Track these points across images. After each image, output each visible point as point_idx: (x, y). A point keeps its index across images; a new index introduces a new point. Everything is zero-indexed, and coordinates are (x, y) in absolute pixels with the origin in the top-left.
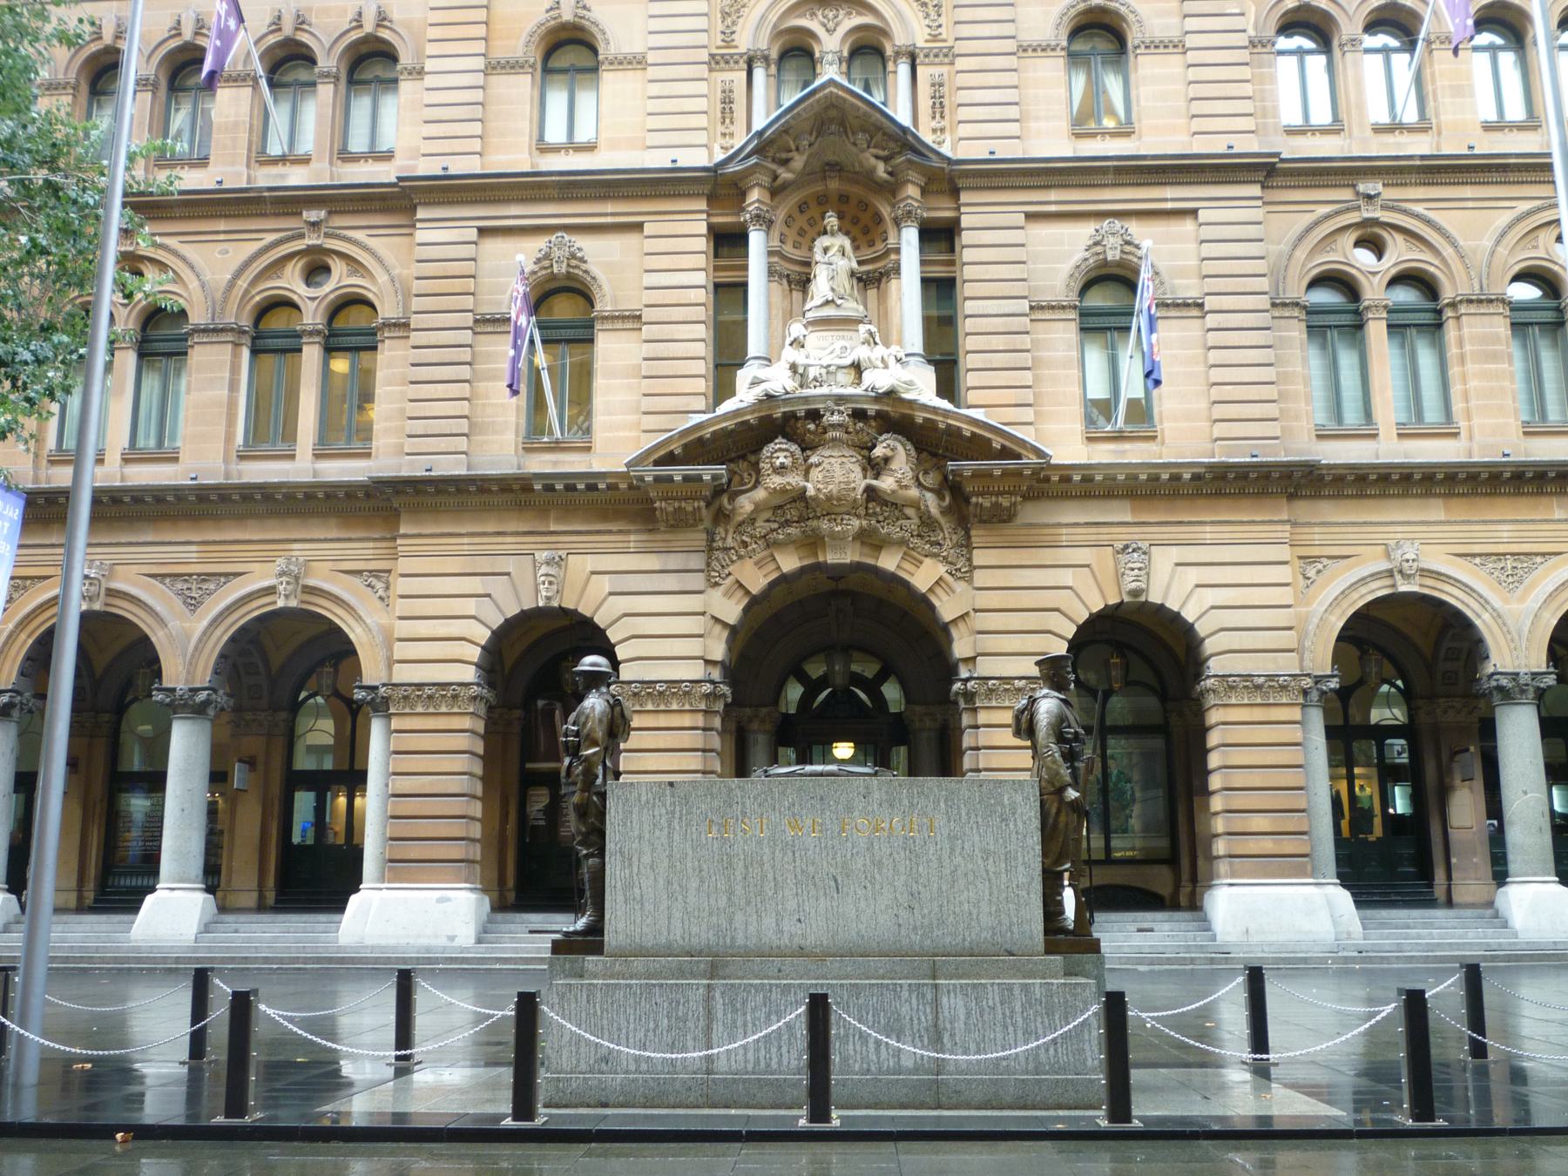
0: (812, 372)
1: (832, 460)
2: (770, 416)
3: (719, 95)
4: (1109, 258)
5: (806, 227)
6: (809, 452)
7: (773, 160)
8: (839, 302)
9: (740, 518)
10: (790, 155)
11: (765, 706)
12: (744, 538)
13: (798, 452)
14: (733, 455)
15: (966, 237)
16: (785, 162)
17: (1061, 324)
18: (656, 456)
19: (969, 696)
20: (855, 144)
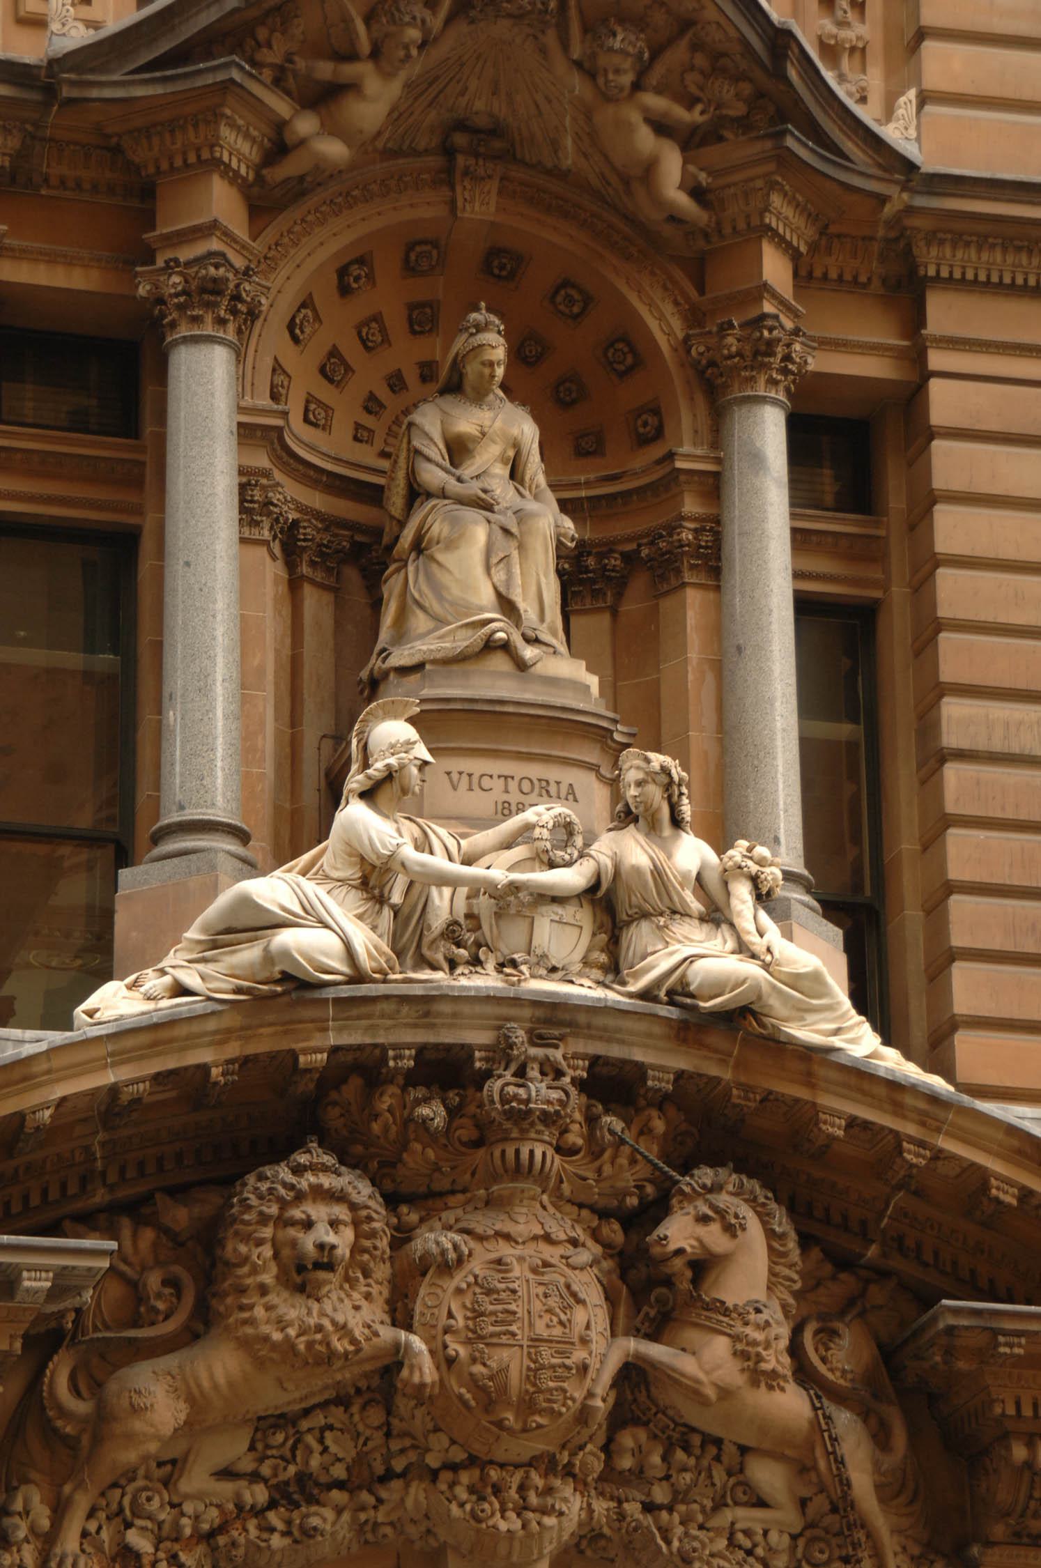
0: (442, 904)
1: (504, 1250)
2: (294, 1055)
5: (352, 350)
7: (278, 82)
9: (130, 1456)
10: (349, 70)
14: (100, 1197)
20: (587, 69)
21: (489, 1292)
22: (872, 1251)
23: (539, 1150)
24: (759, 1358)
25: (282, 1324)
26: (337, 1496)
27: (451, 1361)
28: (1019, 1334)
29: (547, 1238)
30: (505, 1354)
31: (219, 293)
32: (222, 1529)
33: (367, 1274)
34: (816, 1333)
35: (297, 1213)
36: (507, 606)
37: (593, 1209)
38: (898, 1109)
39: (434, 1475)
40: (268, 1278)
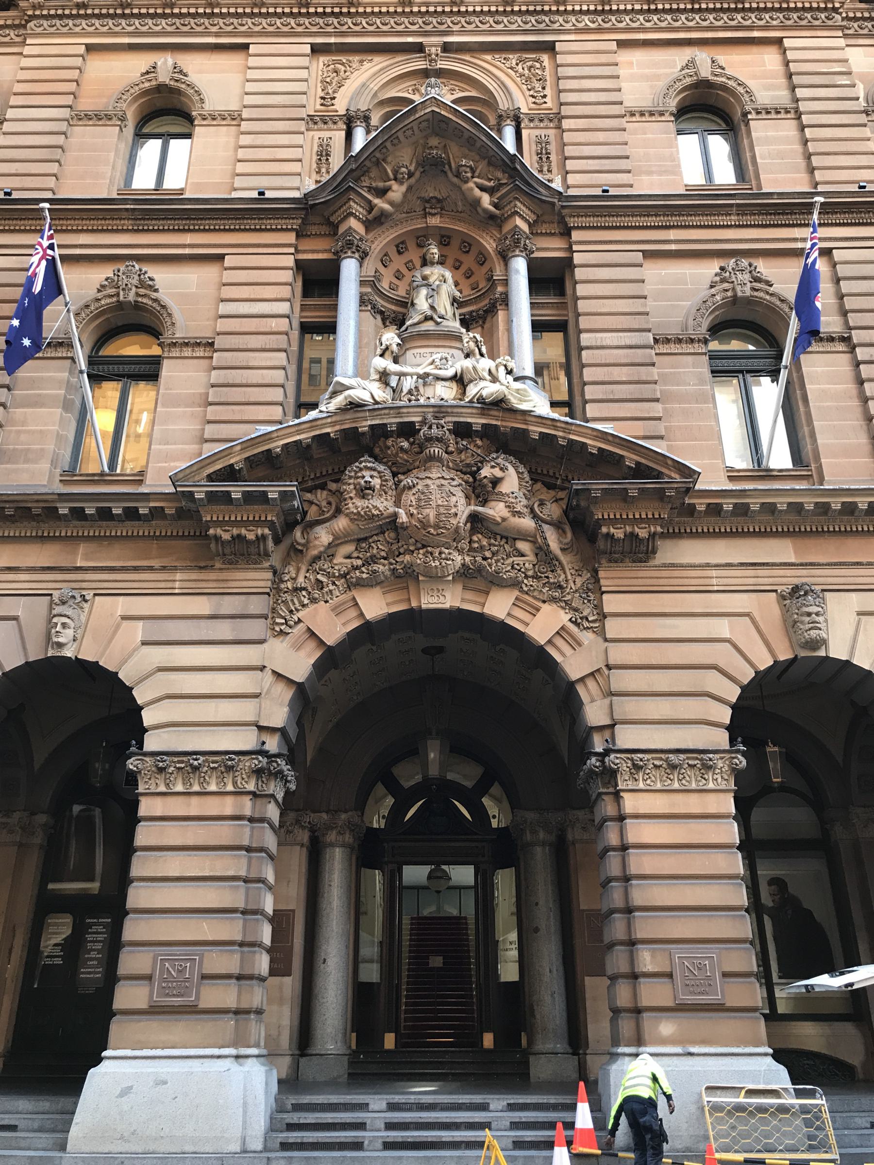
1: (429, 482)
2: (357, 428)
3: (315, 149)
4: (740, 294)
5: (404, 270)
6: (401, 477)
8: (439, 320)
9: (315, 552)
10: (388, 183)
11: (346, 811)
12: (319, 577)
13: (388, 474)
14: (310, 484)
15: (579, 274)
16: (382, 193)
17: (690, 358)
18: (211, 470)
19: (611, 774)
21: (423, 493)
22: (559, 482)
23: (436, 450)
24: (514, 508)
25: (357, 507)
26: (382, 560)
27: (412, 515)
28: (598, 489)
29: (443, 478)
30: (428, 510)
31: (352, 244)
32: (348, 573)
33: (386, 493)
34: (539, 505)
35: (360, 474)
36: (432, 308)
37: (461, 471)
38: (556, 428)
39: (413, 552)
40: (352, 495)
